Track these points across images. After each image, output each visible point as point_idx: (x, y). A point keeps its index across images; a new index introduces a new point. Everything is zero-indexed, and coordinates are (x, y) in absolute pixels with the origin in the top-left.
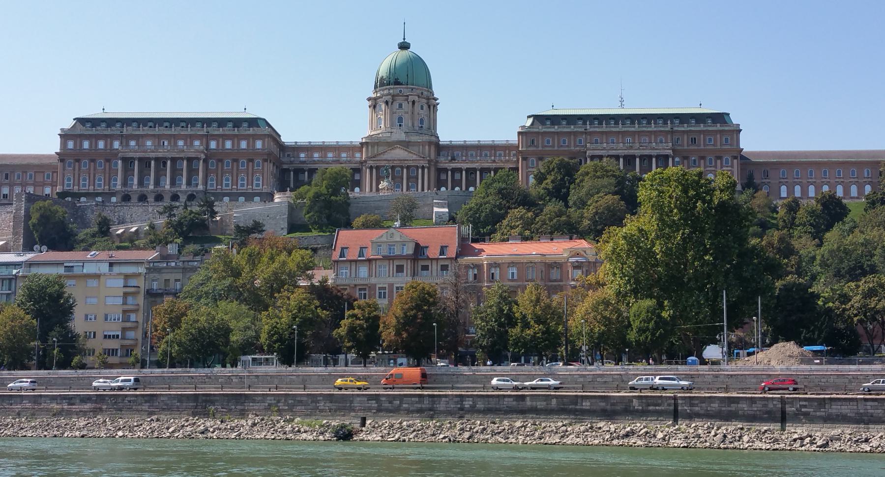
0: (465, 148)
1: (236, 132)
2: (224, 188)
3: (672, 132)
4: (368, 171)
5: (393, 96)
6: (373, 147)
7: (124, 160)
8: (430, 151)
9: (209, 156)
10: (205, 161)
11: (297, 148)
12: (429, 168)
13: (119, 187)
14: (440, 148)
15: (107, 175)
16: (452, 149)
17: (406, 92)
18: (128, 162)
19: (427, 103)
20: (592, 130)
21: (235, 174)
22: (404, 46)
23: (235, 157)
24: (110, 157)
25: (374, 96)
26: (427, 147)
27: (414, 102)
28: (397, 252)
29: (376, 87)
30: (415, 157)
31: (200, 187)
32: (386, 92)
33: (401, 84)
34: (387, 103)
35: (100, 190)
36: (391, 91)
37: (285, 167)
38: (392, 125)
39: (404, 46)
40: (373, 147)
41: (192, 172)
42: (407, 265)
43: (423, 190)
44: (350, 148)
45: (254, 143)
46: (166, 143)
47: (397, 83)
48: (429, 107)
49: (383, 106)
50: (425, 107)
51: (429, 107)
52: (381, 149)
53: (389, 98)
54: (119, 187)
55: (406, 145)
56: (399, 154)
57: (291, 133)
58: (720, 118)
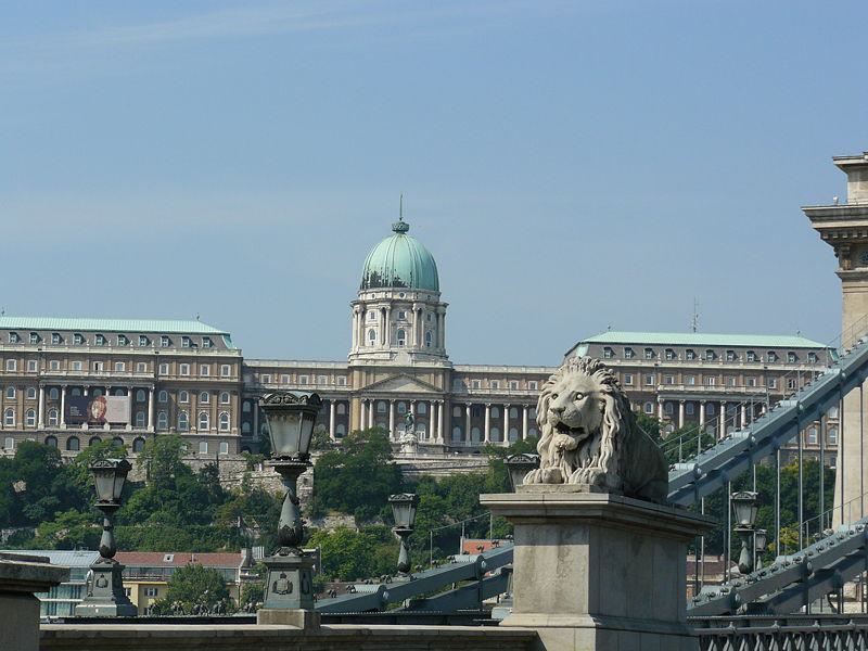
1: (195, 354)
2: (179, 429)
4: (363, 405)
5: (392, 302)
6: (368, 373)
8: (444, 382)
9: (160, 386)
10: (156, 393)
12: (443, 405)
13: (41, 427)
15: (21, 408)
19: (435, 311)
20: (664, 365)
21: (194, 410)
26: (441, 376)
27: (420, 312)
29: (362, 287)
30: (425, 391)
32: (381, 296)
33: (403, 286)
34: (384, 311)
36: (389, 296)
37: (247, 395)
38: (391, 345)
40: (368, 373)
43: (436, 436)
45: (219, 369)
46: (101, 366)
48: (437, 316)
49: (379, 315)
50: (433, 317)
51: (437, 316)
52: (379, 378)
53: (387, 306)
55: (411, 373)
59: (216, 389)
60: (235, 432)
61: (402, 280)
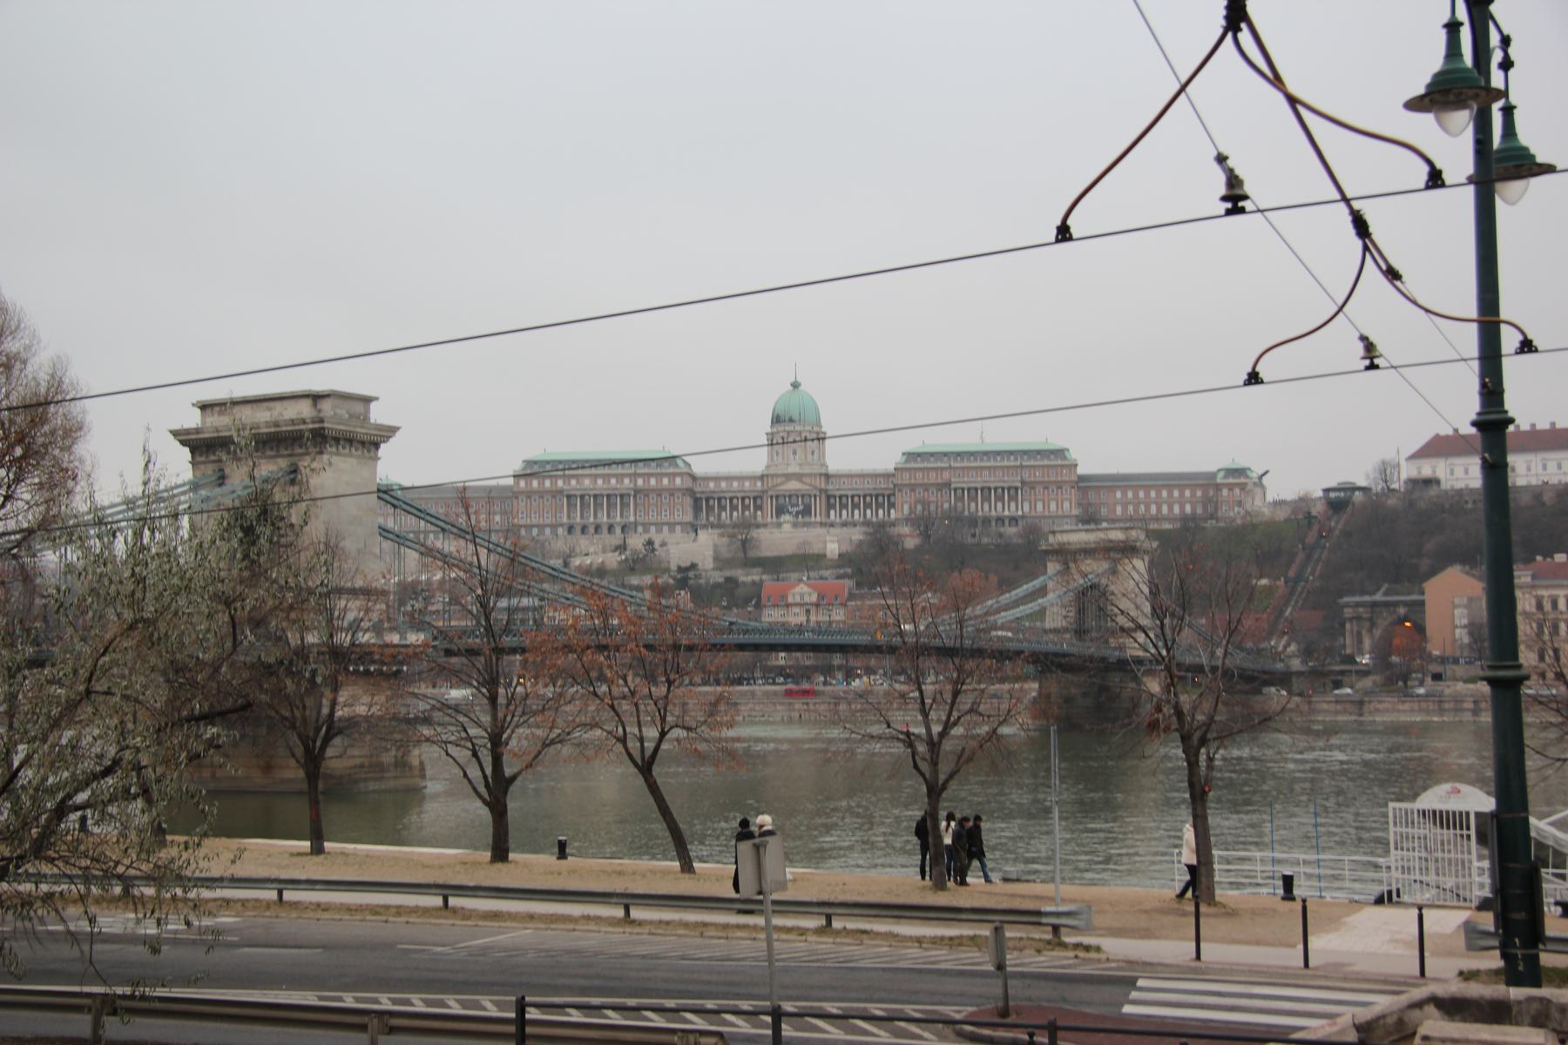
0: (850, 476)
3: (1022, 467)
7: (569, 497)
9: (637, 491)
11: (707, 479)
13: (565, 520)
14: (827, 476)
16: (839, 476)
17: (798, 428)
18: (569, 497)
22: (795, 385)
23: (659, 492)
24: (557, 493)
25: (769, 430)
28: (807, 599)
31: (632, 519)
35: (548, 522)
39: (795, 385)
41: (624, 505)
42: (813, 610)
44: (753, 478)
47: (791, 420)
54: (565, 520)
55: (799, 477)
56: (793, 485)
57: (700, 467)
58: (1060, 453)
59: (672, 492)
60: (689, 517)
61: (796, 417)
